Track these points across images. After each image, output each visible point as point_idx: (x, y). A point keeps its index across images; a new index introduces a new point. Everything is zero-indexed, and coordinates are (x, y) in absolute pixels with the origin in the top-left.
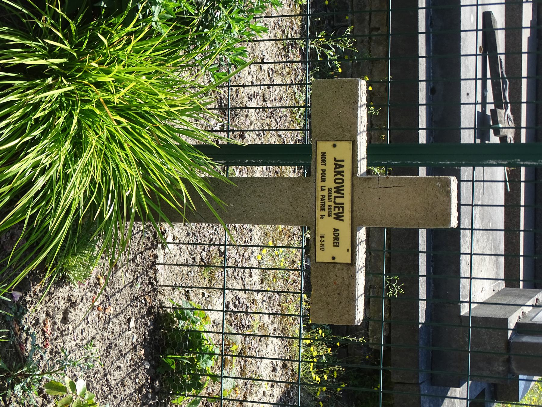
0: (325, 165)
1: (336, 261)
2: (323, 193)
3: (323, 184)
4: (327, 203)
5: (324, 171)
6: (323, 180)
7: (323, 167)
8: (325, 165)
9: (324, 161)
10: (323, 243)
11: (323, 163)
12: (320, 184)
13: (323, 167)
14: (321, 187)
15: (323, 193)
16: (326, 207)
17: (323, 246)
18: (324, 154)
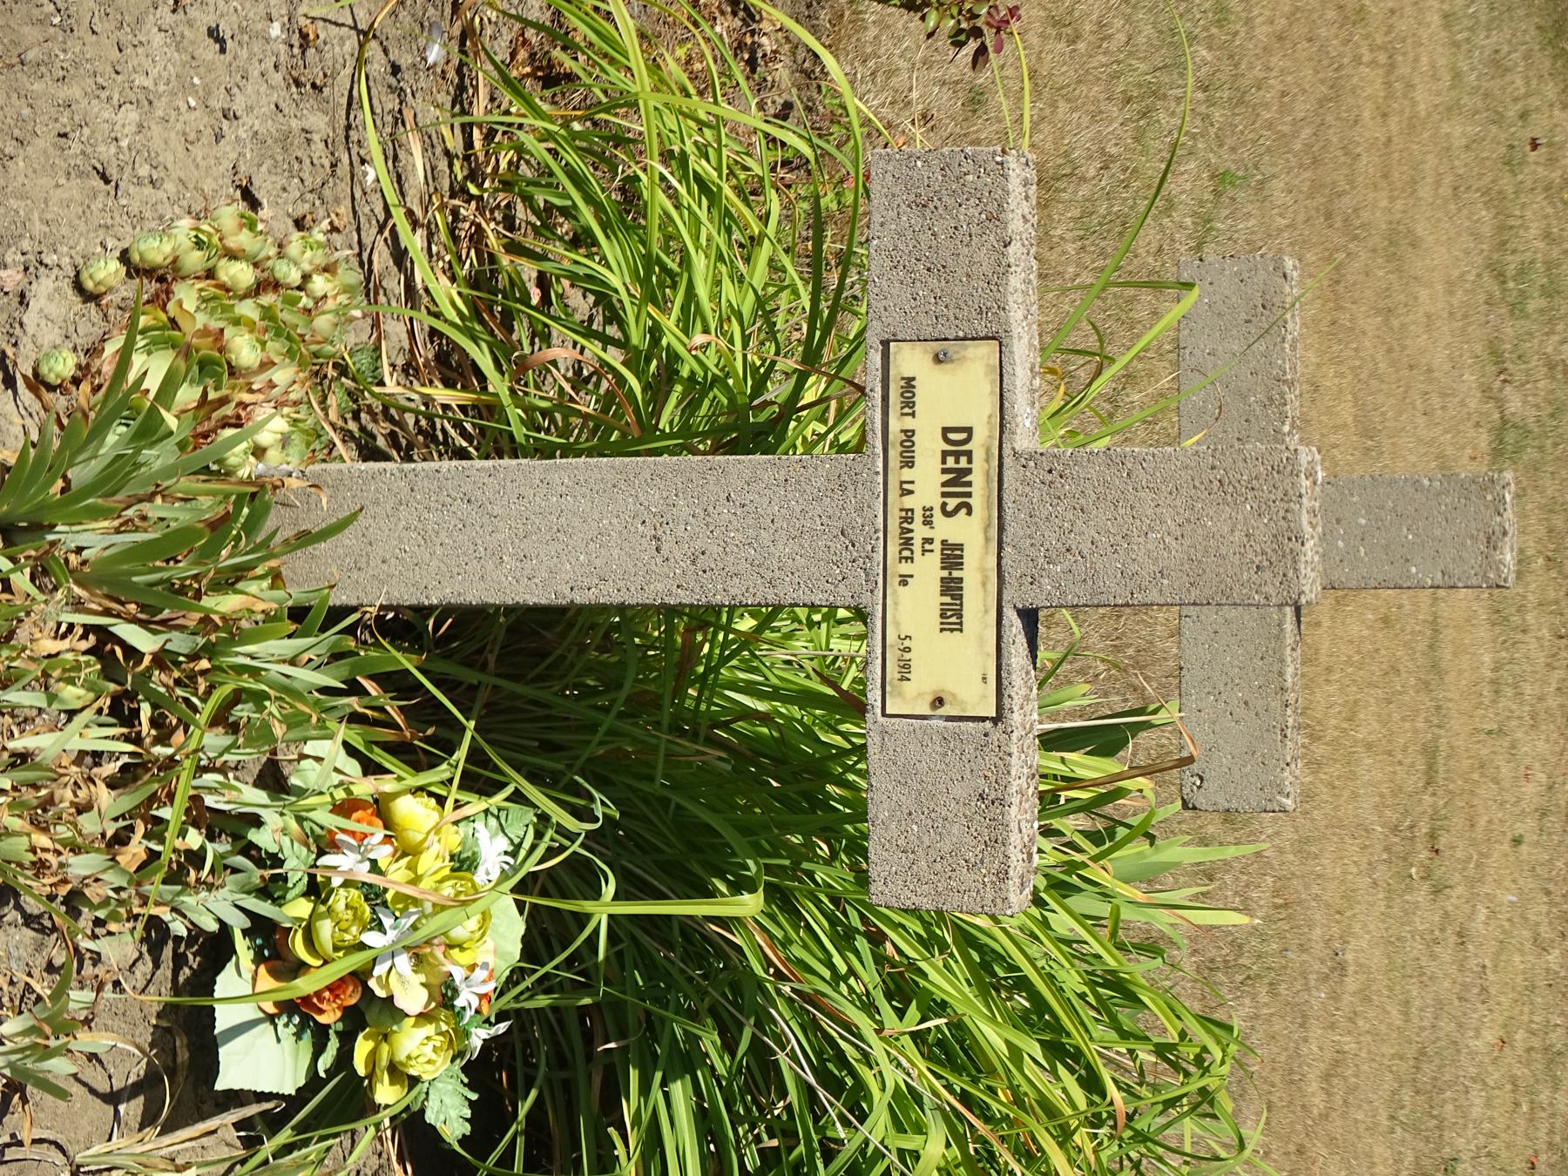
0: (913, 415)
1: (946, 710)
2: (908, 502)
3: (907, 474)
4: (919, 531)
5: (909, 434)
6: (909, 463)
7: (909, 423)
8: (913, 415)
9: (909, 404)
10: (907, 656)
11: (907, 410)
12: (898, 474)
13: (909, 423)
14: (902, 482)
15: (908, 502)
16: (917, 547)
17: (905, 666)
18: (909, 382)
